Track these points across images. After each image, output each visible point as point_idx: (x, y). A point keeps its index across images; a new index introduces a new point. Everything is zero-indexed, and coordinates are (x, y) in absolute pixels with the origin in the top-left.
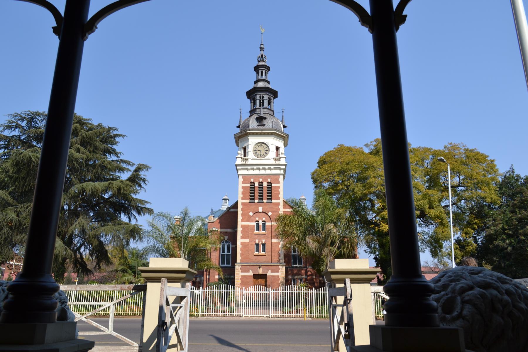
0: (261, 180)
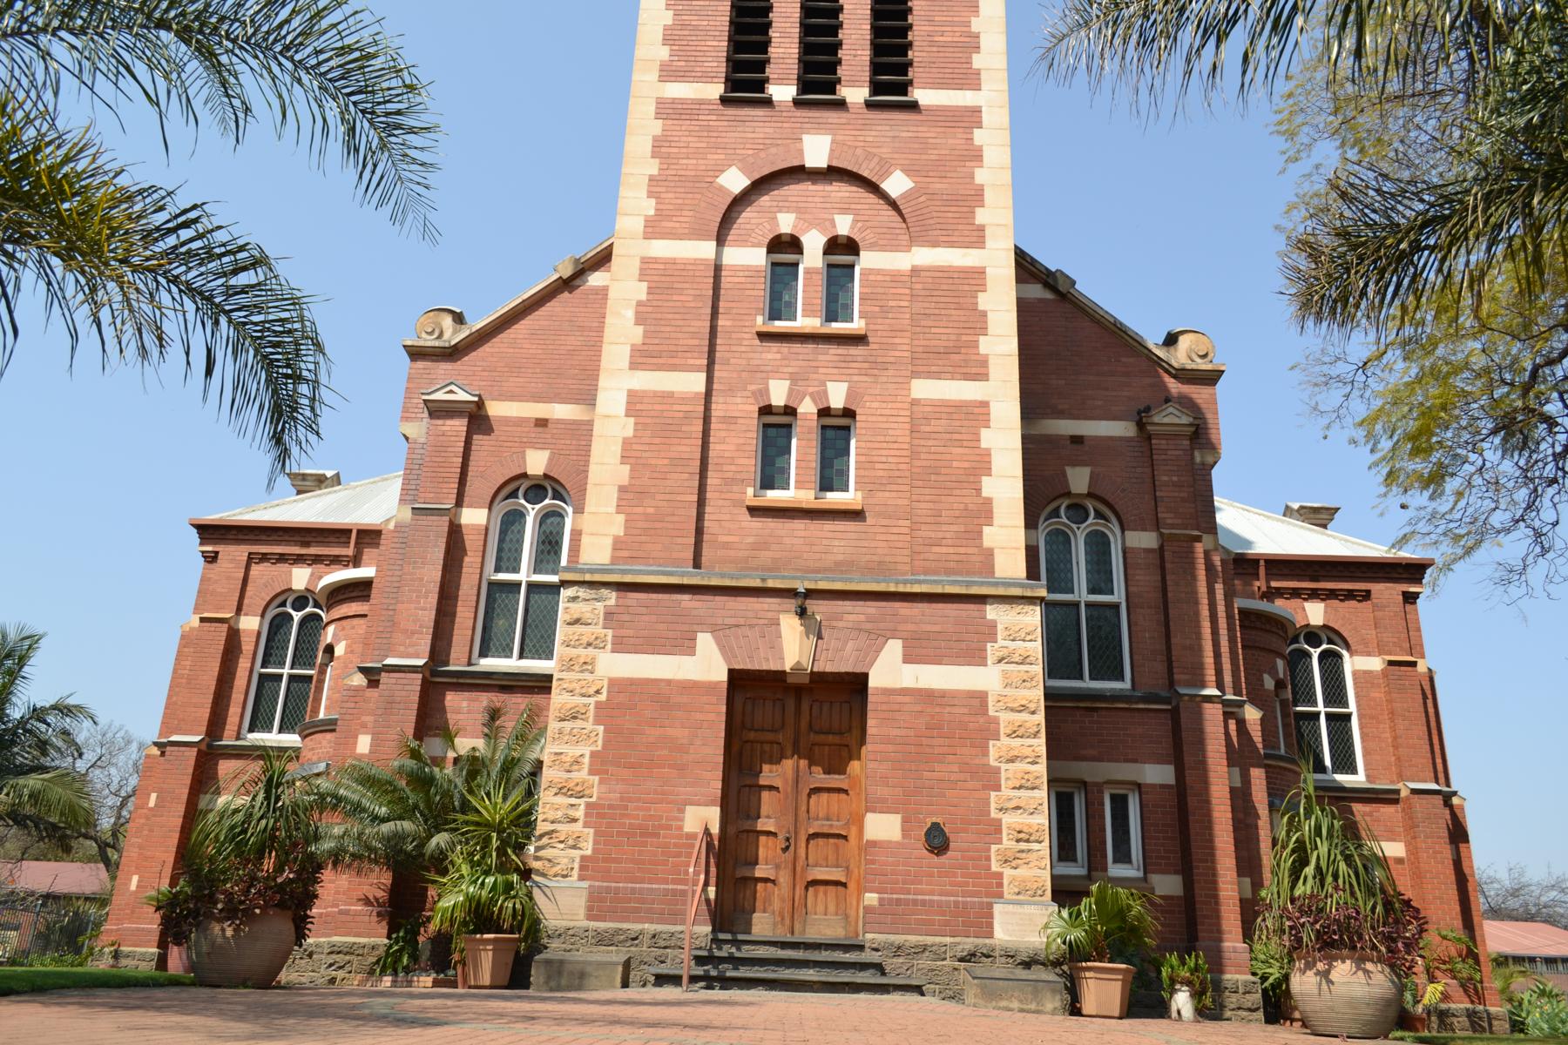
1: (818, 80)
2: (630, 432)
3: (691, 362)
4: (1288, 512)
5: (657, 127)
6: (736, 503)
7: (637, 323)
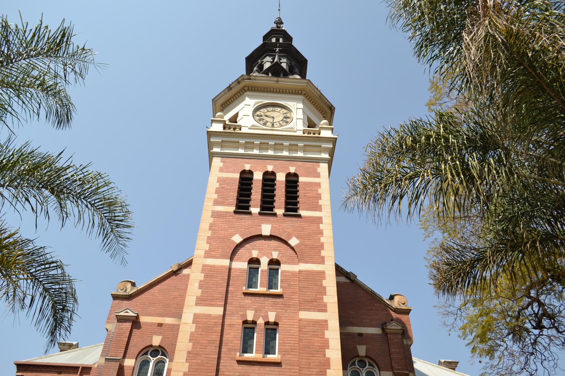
0: (270, 168)
1: (267, 206)
2: (193, 330)
3: (218, 303)
4: (440, 363)
5: (211, 220)
6: (232, 359)
7: (199, 288)
